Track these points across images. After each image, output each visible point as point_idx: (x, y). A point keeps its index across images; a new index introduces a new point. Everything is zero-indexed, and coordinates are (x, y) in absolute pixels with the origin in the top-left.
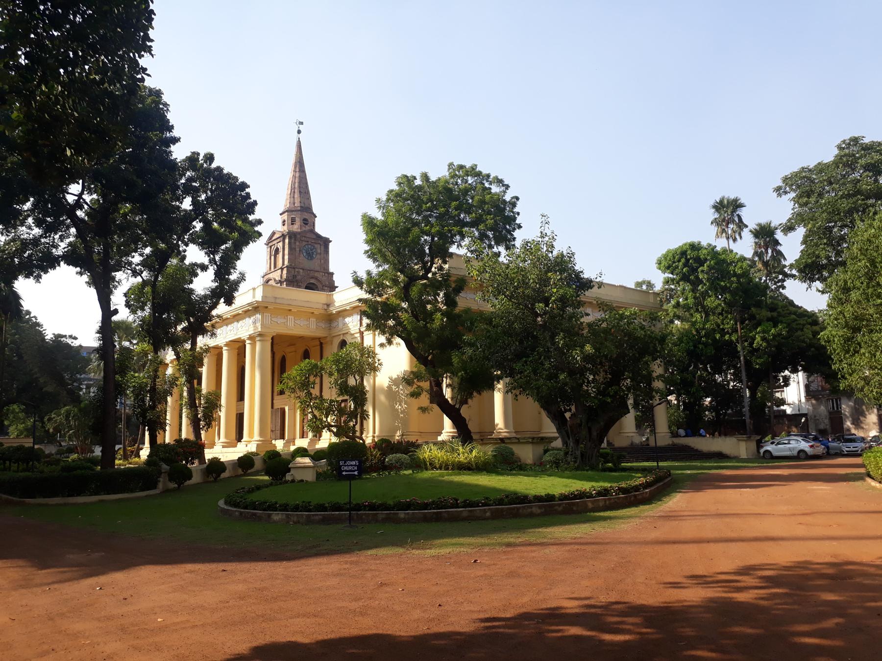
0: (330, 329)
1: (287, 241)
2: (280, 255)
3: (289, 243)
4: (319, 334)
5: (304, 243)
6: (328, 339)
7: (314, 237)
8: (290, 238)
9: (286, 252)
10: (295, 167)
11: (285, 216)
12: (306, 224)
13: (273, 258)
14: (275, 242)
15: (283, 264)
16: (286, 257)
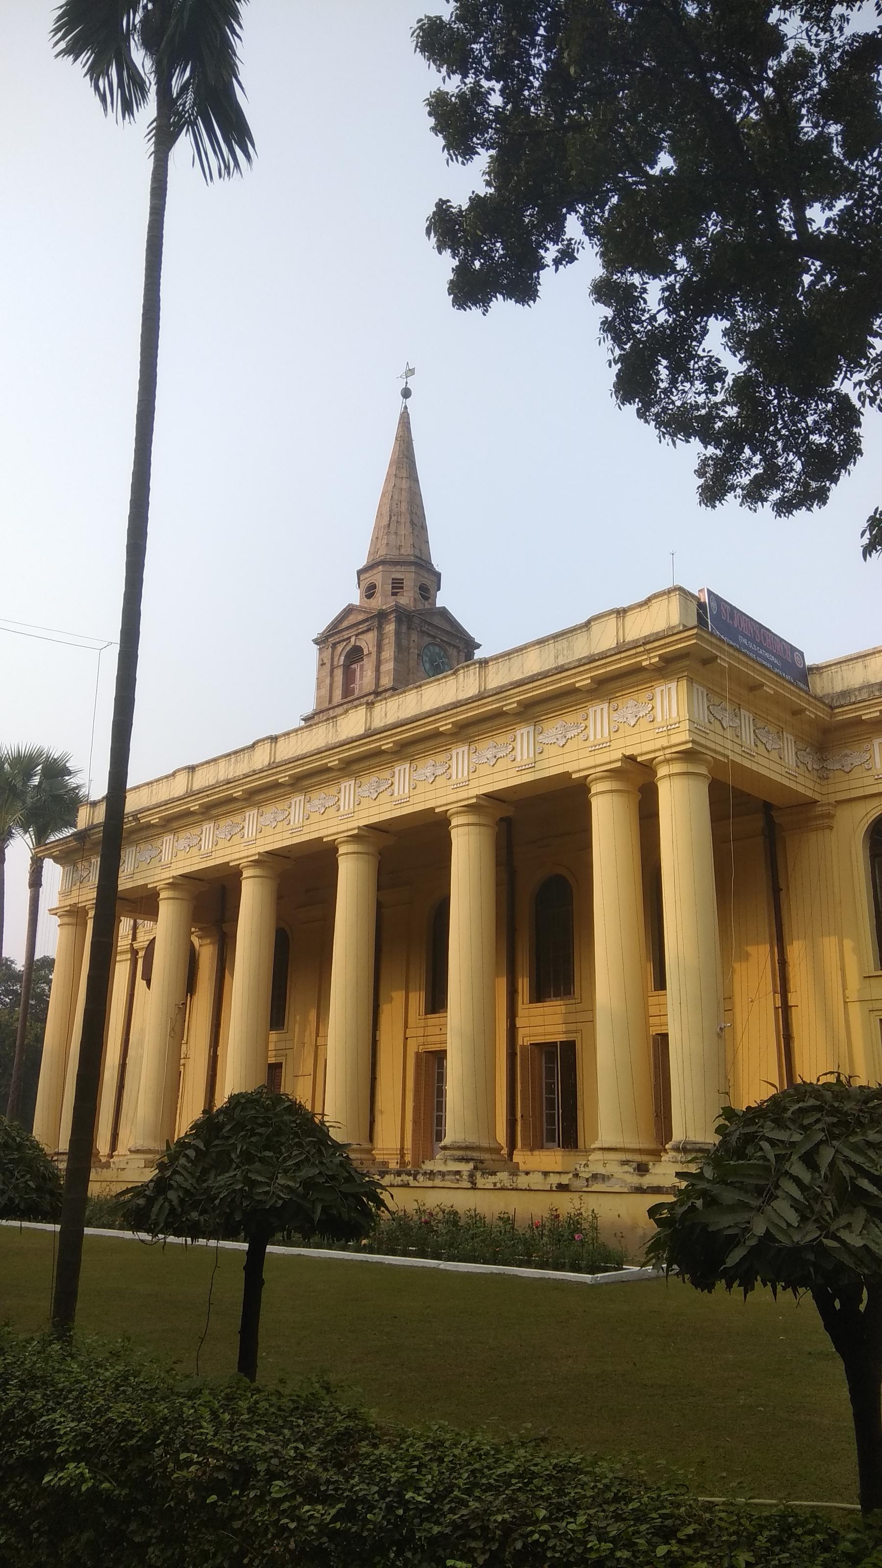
0: (823, 775)
1: (390, 628)
2: (368, 664)
3: (398, 633)
4: (803, 784)
5: (427, 640)
6: (819, 810)
7: (449, 629)
8: (399, 621)
9: (389, 653)
10: (398, 468)
11: (377, 577)
12: (426, 598)
13: (339, 674)
14: (346, 635)
15: (377, 684)
16: (388, 667)
